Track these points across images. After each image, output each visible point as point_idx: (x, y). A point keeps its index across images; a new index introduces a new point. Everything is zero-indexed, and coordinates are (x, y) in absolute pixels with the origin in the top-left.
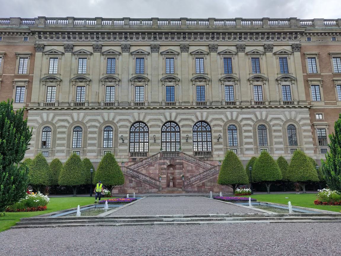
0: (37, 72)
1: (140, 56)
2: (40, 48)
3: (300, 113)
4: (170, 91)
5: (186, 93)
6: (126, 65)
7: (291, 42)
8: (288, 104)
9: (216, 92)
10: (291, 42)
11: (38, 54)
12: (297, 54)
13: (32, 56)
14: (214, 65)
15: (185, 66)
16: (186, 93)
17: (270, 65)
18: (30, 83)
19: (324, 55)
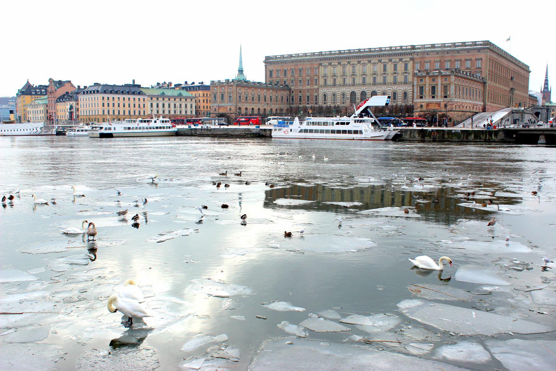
0: (320, 75)
1: (354, 66)
2: (321, 64)
4: (364, 79)
5: (369, 80)
6: (349, 69)
7: (410, 57)
8: (405, 83)
9: (380, 79)
10: (410, 57)
11: (320, 67)
12: (412, 62)
13: (319, 67)
14: (379, 68)
15: (369, 69)
16: (369, 80)
17: (401, 67)
18: (319, 78)
19: (422, 62)
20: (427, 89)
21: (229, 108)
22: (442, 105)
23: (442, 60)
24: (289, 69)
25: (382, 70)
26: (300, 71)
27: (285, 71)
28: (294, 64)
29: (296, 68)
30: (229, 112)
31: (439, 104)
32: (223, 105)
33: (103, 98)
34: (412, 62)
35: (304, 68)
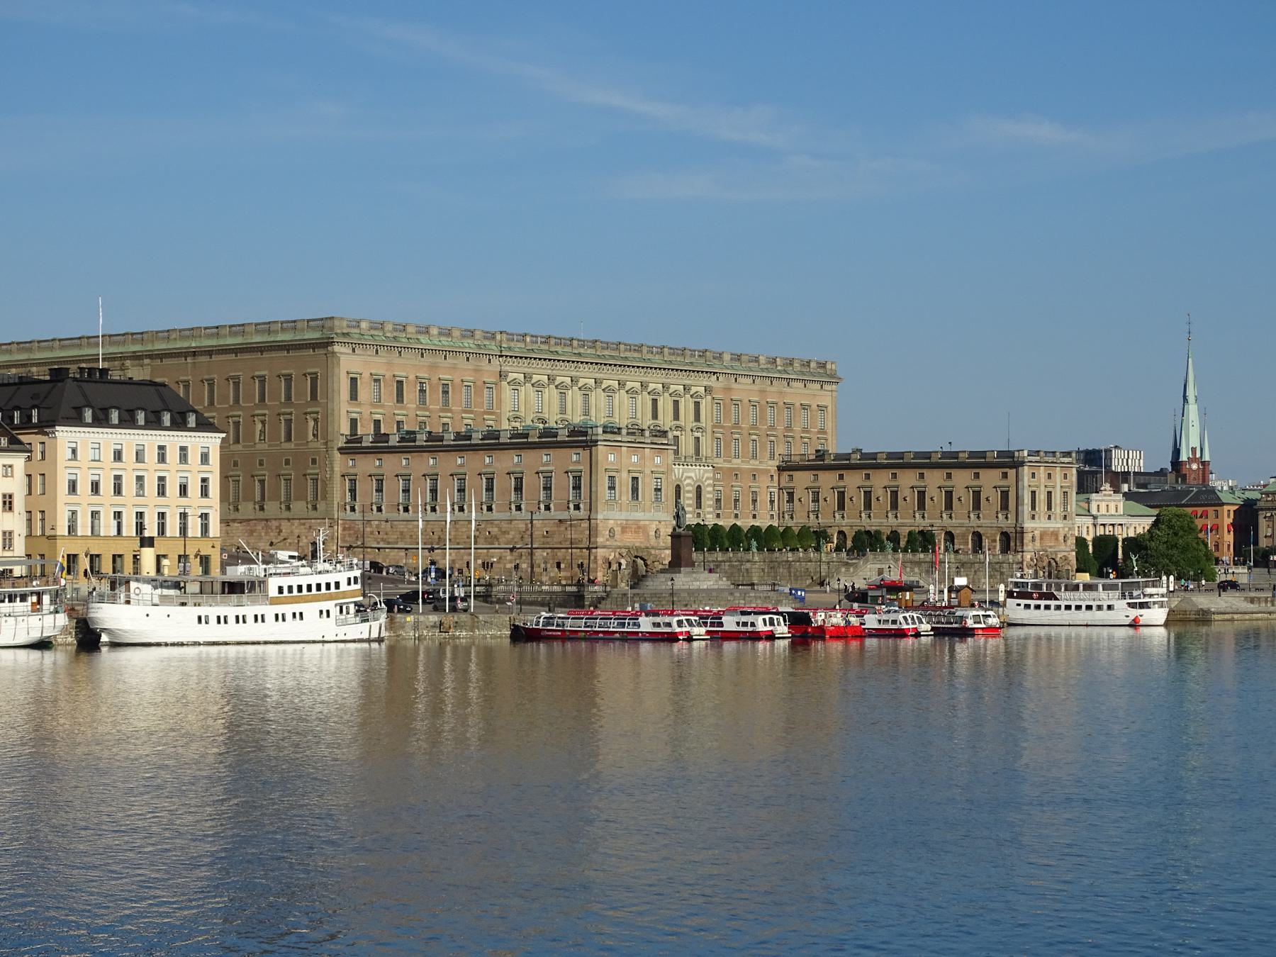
3: (706, 471)
7: (705, 383)
11: (504, 383)
12: (709, 397)
20: (1042, 497)
21: (654, 527)
22: (1061, 538)
23: (763, 402)
24: (412, 377)
25: (650, 415)
26: (446, 392)
27: (400, 383)
28: (428, 359)
29: (435, 380)
30: (653, 542)
31: (1055, 534)
32: (638, 515)
33: (118, 456)
34: (709, 397)
35: (457, 381)
